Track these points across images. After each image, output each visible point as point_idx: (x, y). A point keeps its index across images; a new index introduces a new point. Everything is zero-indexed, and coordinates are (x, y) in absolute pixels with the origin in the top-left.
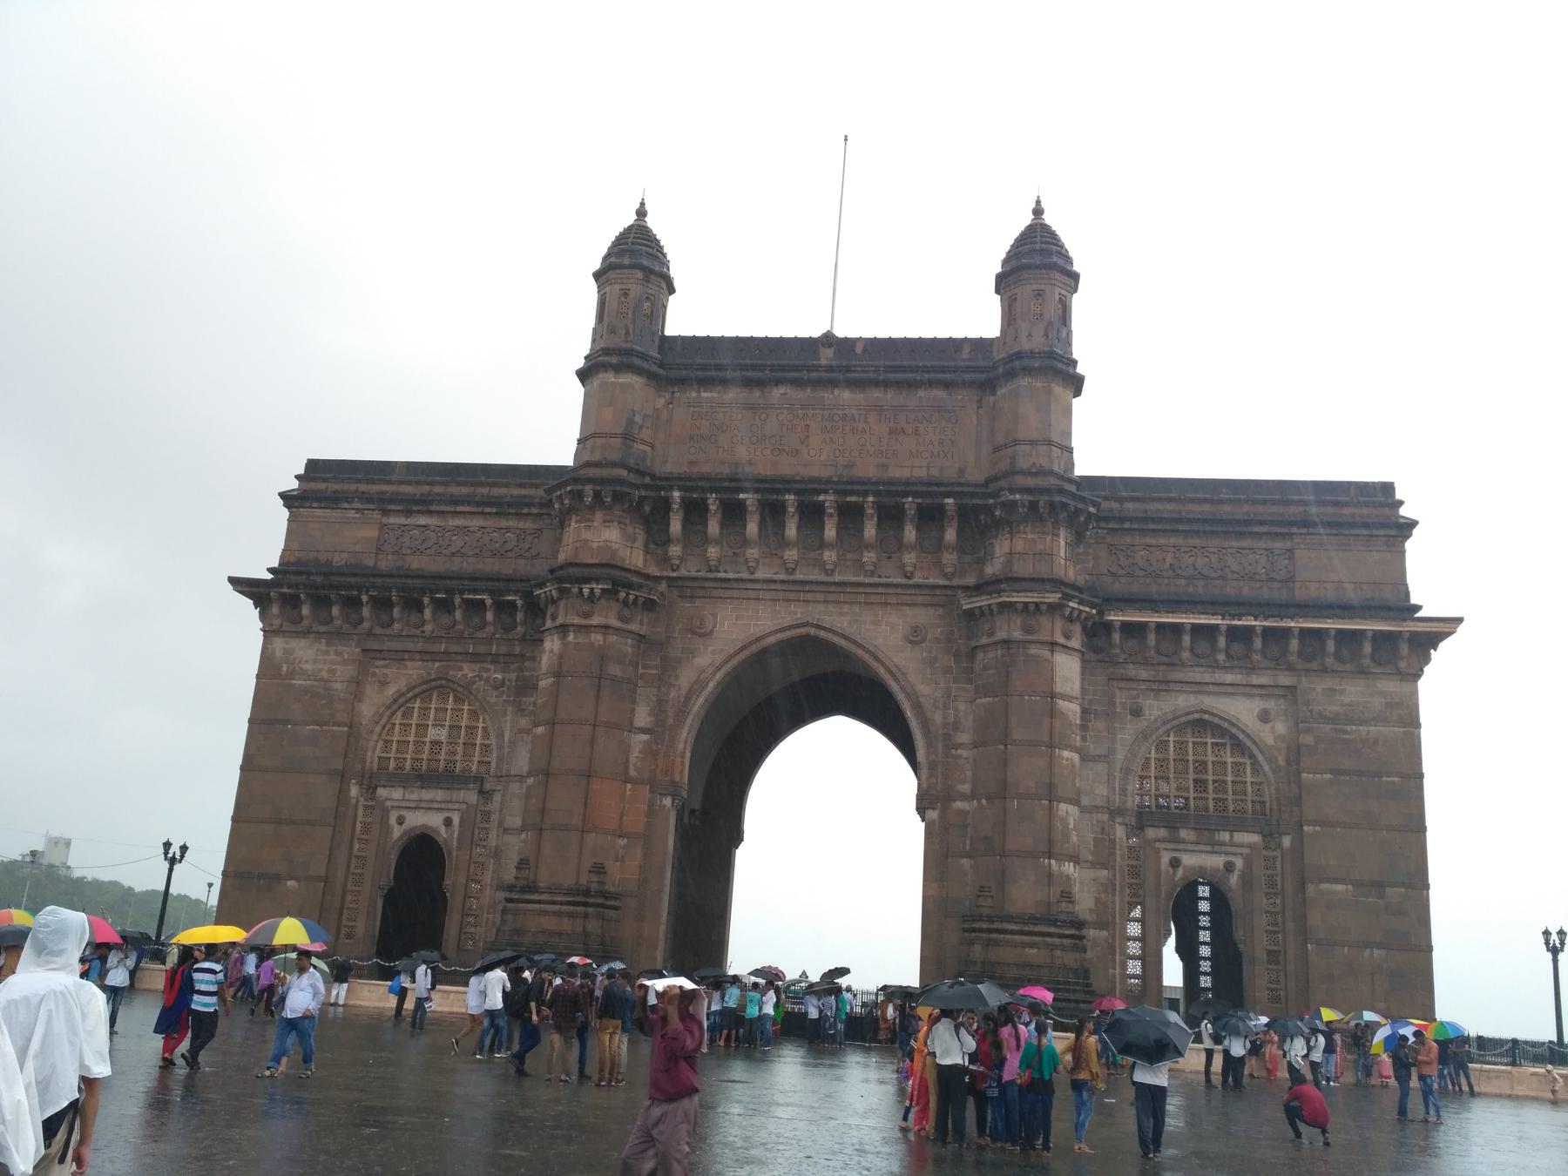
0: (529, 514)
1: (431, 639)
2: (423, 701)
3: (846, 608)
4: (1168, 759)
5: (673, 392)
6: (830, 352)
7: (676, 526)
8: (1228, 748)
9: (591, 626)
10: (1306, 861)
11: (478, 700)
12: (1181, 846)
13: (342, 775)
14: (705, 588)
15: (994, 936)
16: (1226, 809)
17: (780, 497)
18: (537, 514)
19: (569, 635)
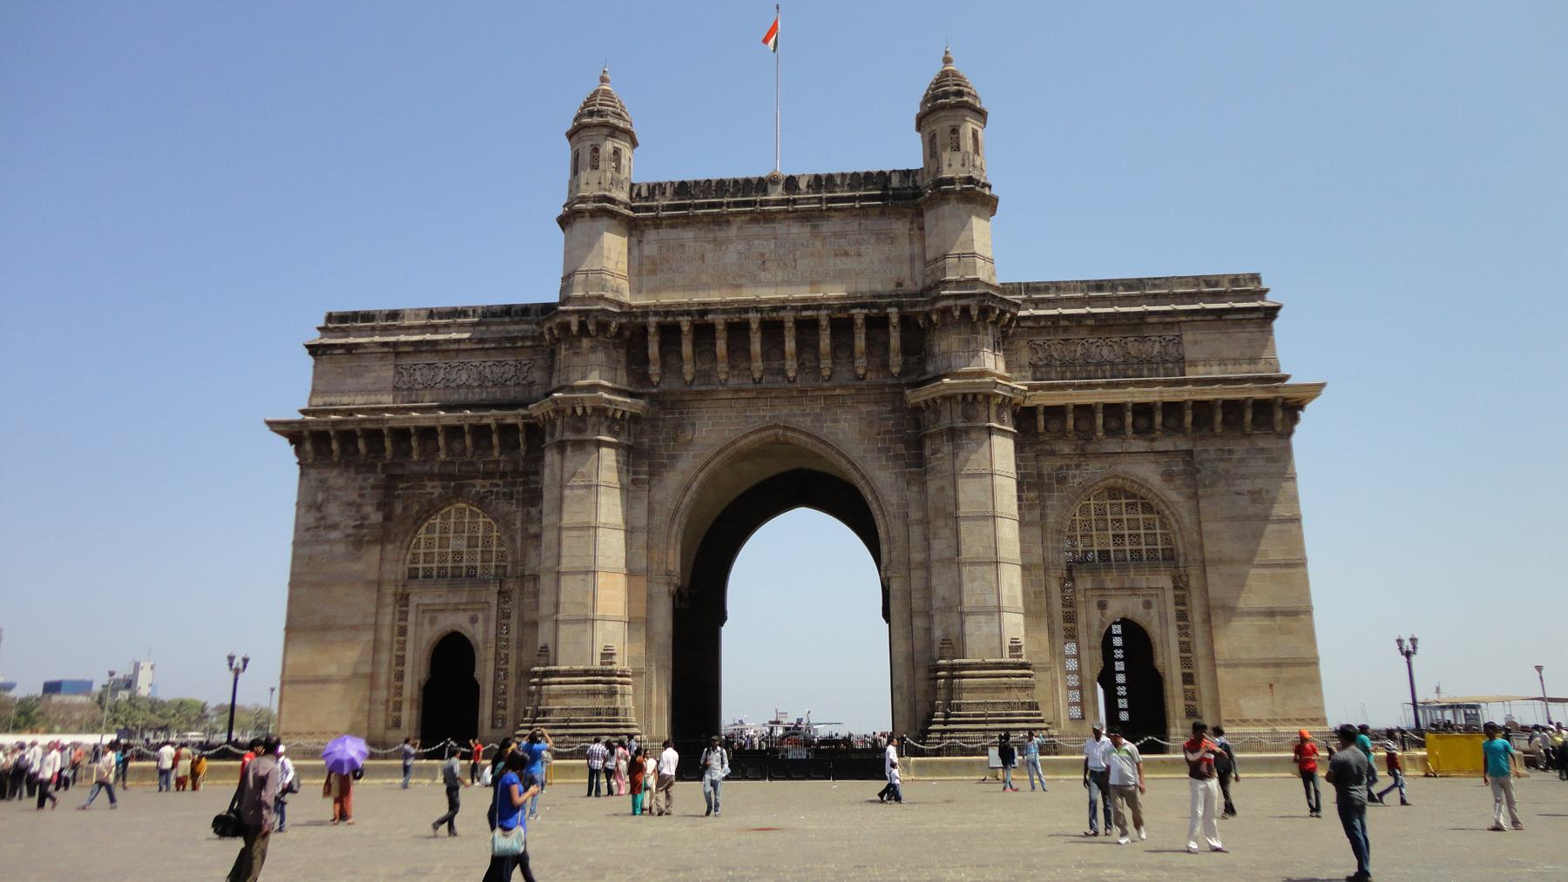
0: (522, 347)
1: (444, 463)
4: (1091, 520)
5: (642, 232)
6: (780, 188)
7: (653, 350)
8: (1139, 506)
9: (585, 441)
10: (1210, 595)
12: (1107, 593)
13: (379, 585)
14: (684, 401)
16: (1141, 559)
18: (527, 347)
19: (566, 449)
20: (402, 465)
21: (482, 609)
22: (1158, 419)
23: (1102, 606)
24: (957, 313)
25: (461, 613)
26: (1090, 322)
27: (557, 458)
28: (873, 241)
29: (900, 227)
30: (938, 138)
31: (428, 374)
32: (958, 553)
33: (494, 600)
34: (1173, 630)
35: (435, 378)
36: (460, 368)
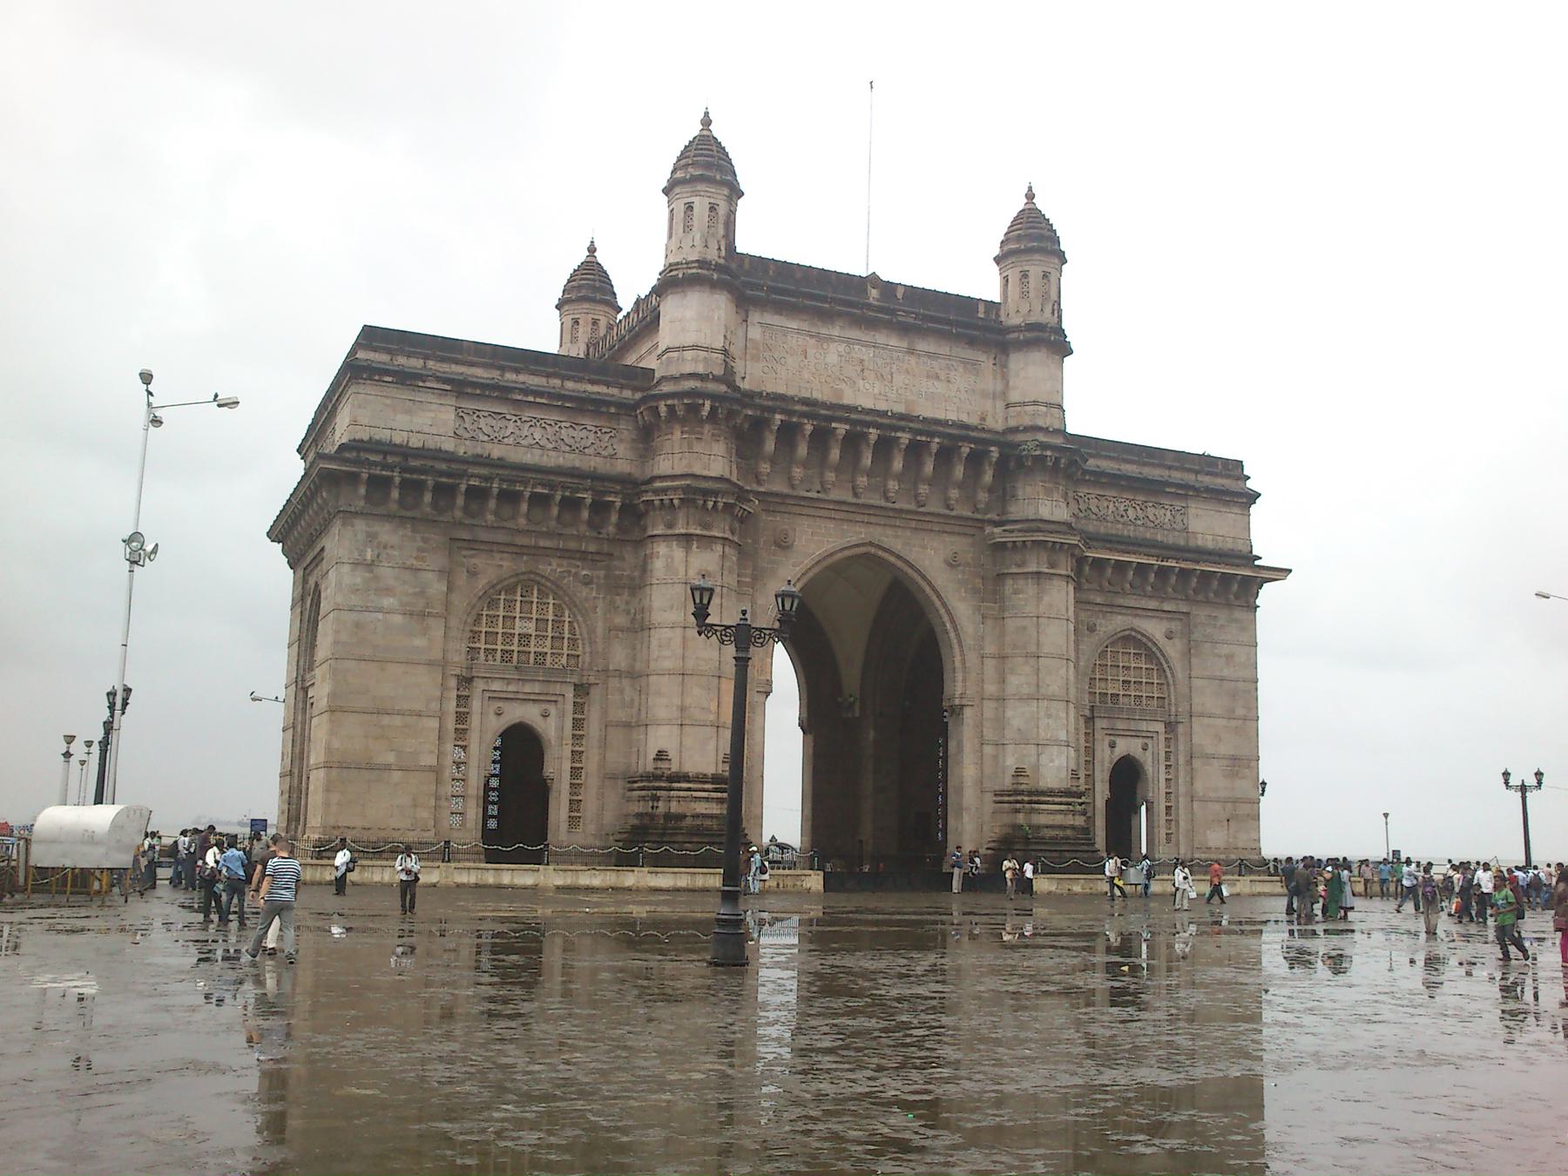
2: (506, 592)
3: (900, 532)
5: (747, 312)
7: (770, 445)
8: (1143, 656)
11: (568, 595)
15: (1036, 806)
17: (865, 430)
22: (1173, 579)
23: (1112, 746)
24: (1050, 464)
25: (531, 704)
26: (1123, 483)
27: (678, 553)
29: (985, 360)
30: (1032, 280)
31: (498, 424)
32: (1038, 685)
33: (570, 694)
34: (1162, 768)
35: (503, 431)
36: (532, 423)
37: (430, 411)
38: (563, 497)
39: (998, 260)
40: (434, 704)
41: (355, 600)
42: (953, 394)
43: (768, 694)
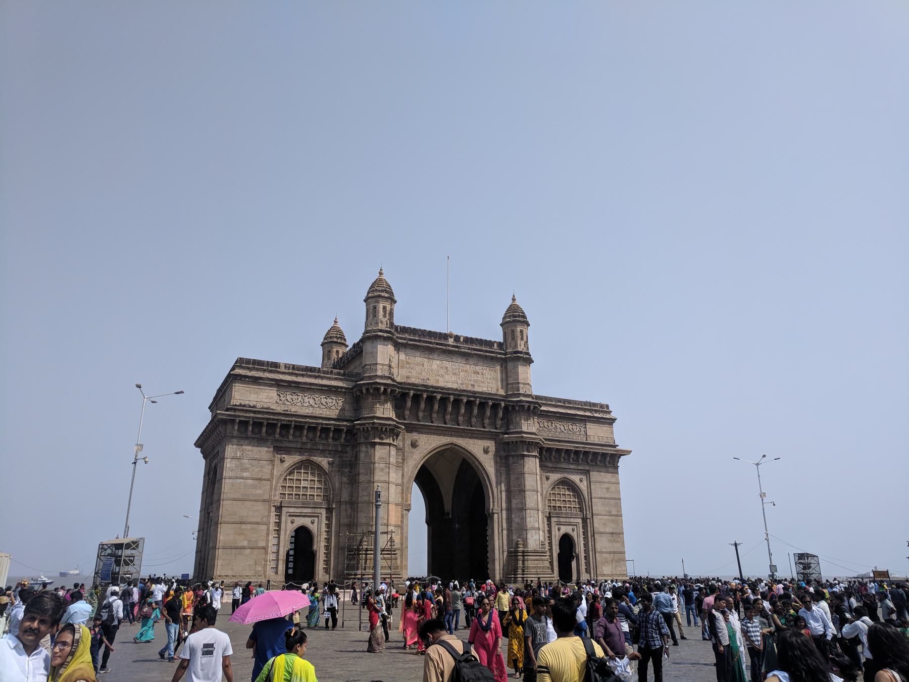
1: (303, 443)
7: (409, 404)
20: (281, 441)
21: (318, 517)
23: (559, 530)
28: (488, 370)
33: (324, 512)
34: (582, 539)
37: (266, 392)
38: (322, 428)
39: (501, 325)
40: (265, 519)
41: (231, 474)
42: (485, 380)
43: (408, 510)
